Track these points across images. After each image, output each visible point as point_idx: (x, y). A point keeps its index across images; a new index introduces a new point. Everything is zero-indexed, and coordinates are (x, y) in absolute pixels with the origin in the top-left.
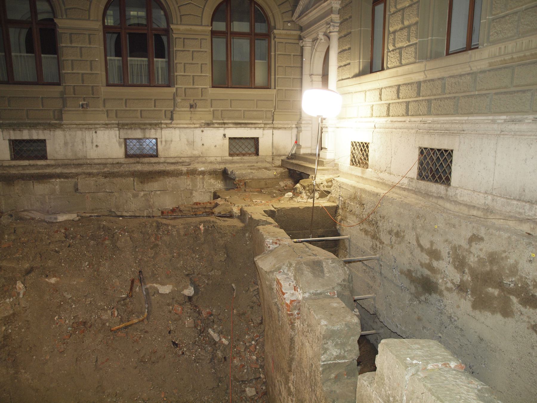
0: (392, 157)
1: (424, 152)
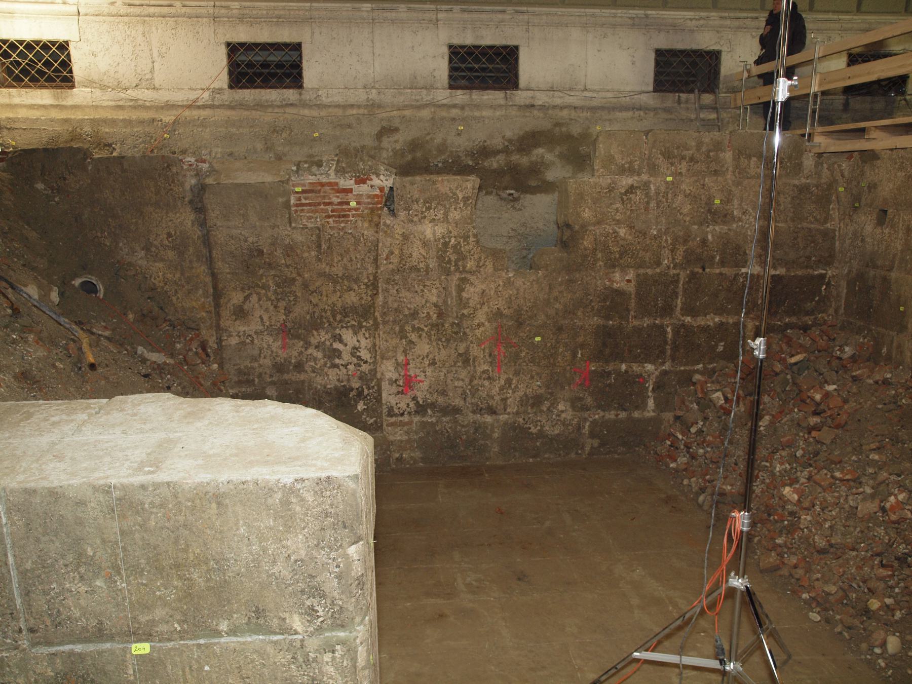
0: (153, 62)
1: (233, 49)
